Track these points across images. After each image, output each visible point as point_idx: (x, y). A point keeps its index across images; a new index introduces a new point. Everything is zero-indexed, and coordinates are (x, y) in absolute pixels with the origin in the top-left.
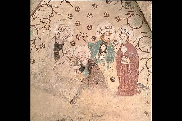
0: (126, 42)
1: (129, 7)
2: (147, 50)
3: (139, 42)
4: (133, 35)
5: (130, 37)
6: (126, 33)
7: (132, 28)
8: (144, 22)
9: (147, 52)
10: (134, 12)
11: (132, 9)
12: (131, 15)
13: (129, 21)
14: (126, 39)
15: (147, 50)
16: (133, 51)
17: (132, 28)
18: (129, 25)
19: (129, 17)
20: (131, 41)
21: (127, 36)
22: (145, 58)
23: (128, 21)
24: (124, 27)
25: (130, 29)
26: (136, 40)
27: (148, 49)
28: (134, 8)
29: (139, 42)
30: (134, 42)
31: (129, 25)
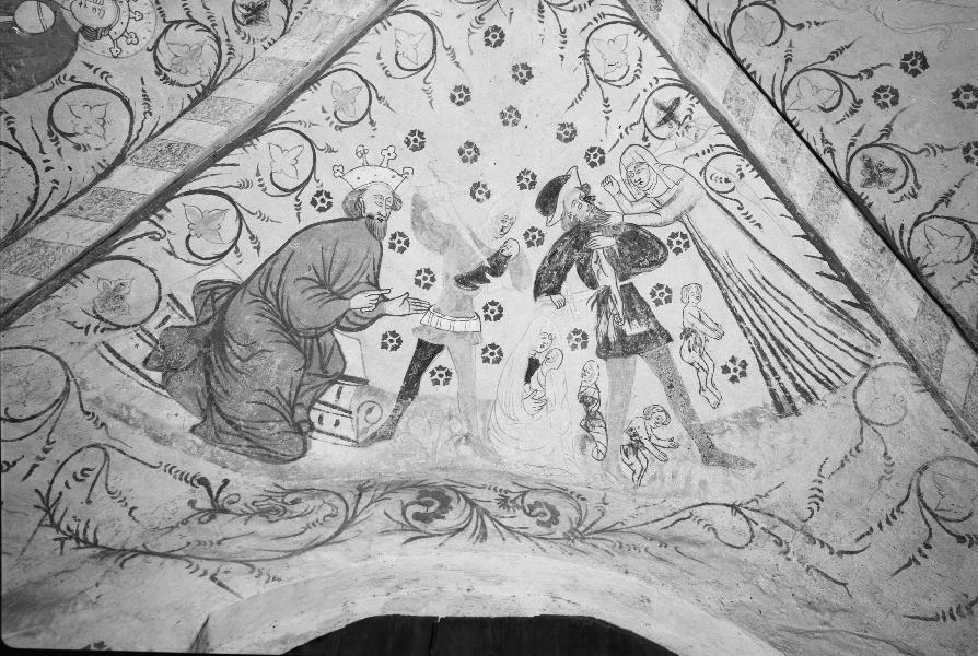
0: (76, 27)
1: (241, 20)
2: (63, 134)
3: (94, 86)
4: (124, 54)
5: (106, 41)
6: (124, 19)
7: (156, 47)
8: (197, 92)
9: (51, 134)
10: (228, 40)
11: (238, 31)
12: (209, 31)
13: (183, 25)
14: (94, 22)
15: (63, 134)
16: (35, 64)
17: (156, 47)
18: (166, 31)
19: (197, 23)
20: (87, 52)
21: (110, 28)
22: (13, 131)
23: (179, 22)
24: (151, 9)
25: (148, 36)
26: (99, 72)
27: (71, 135)
28: (243, 39)
29: (94, 86)
30: (91, 67)
31: (166, 31)
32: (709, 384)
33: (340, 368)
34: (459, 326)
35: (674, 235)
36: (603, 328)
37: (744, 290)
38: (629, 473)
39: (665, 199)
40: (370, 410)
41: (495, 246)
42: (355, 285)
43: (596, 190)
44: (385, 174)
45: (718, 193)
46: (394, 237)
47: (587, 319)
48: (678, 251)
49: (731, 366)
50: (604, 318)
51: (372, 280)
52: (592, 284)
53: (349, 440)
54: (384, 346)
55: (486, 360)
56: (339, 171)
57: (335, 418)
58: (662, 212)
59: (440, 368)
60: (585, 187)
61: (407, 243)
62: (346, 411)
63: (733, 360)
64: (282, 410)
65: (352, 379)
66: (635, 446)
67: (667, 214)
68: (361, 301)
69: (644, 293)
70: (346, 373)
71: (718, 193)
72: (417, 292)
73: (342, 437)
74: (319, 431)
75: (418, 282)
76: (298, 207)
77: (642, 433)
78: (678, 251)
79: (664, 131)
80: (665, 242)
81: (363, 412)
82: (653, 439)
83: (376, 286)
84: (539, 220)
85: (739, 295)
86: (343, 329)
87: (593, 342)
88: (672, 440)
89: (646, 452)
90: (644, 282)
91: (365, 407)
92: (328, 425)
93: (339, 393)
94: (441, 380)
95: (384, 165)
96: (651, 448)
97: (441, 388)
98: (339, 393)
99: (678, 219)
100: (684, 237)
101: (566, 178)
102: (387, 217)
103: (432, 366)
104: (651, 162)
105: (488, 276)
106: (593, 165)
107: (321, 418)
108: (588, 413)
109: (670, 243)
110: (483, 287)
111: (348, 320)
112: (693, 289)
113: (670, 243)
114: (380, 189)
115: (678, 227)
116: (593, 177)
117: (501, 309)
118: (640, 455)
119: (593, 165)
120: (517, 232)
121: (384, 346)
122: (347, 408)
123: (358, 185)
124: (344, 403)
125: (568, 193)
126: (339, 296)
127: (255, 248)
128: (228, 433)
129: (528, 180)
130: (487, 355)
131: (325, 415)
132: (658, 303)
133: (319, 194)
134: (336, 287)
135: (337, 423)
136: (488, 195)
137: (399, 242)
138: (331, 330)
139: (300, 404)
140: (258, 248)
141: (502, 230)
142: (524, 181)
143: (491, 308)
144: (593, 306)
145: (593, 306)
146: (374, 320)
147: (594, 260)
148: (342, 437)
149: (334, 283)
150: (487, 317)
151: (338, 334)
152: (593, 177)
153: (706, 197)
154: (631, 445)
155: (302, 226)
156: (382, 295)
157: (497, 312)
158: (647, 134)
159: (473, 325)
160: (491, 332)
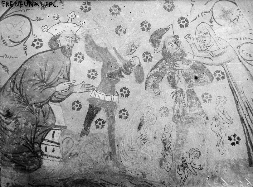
32: (221, 143)
33: (53, 122)
34: (109, 98)
35: (218, 72)
36: (177, 108)
37: (247, 106)
38: (179, 178)
39: (216, 53)
40: (68, 142)
41: (128, 58)
42: (58, 80)
43: (182, 39)
44: (70, 26)
45: (244, 59)
46: (76, 55)
47: (170, 103)
48: (218, 79)
49: (233, 138)
50: (178, 104)
51: (66, 77)
52: (174, 86)
53: (59, 158)
54: (73, 109)
55: (121, 117)
56: (46, 28)
57: (51, 148)
58: (213, 59)
59: (100, 119)
60: (176, 37)
61: (83, 58)
62: (57, 143)
63: (234, 136)
64: (28, 146)
65: (60, 127)
66: (184, 165)
67: (216, 61)
68: (60, 87)
69: (199, 95)
70: (56, 124)
71: (244, 59)
72: (90, 81)
73: (56, 157)
74: (46, 155)
75: (89, 76)
76: (25, 49)
77: (188, 161)
78: (218, 79)
79: (222, 21)
80: (213, 74)
81: (64, 143)
82: (192, 164)
83: (69, 79)
84: (149, 47)
85: (244, 108)
86: (53, 101)
87: (171, 113)
88: (200, 166)
89: (188, 169)
90: (199, 90)
91: (66, 141)
92: (49, 152)
93: (53, 134)
94: (100, 126)
95: (70, 21)
96: (191, 168)
97: (100, 130)
98: (53, 134)
99: (221, 65)
100: (223, 73)
101: (167, 29)
102: (72, 46)
103: (96, 119)
104: (213, 34)
105: (123, 74)
106: (182, 26)
107: (46, 148)
108: (165, 148)
109: (215, 74)
110: (121, 79)
111: (55, 96)
112: (223, 99)
113: (215, 74)
114: (68, 33)
115: (221, 69)
116: (181, 33)
117: (129, 92)
118: (185, 171)
119: (182, 26)
120: (139, 53)
121: (73, 109)
122: (57, 142)
123: (55, 33)
124: (56, 139)
125: (166, 37)
126: (51, 86)
127: (5, 71)
128: (5, 161)
129: (146, 26)
130: (121, 114)
131: (48, 147)
132: (205, 101)
133: (35, 40)
134: (48, 82)
135: (53, 151)
136: (125, 32)
137: (79, 57)
138: (47, 103)
139: (36, 142)
140: (8, 71)
141: (131, 51)
142: (144, 27)
143: (124, 90)
144: (173, 97)
145: (173, 97)
146: (67, 96)
147: (176, 75)
148: (56, 157)
149: (47, 80)
150: (122, 95)
151: (52, 105)
152: (181, 33)
153: (237, 59)
154: (182, 166)
155: (28, 56)
156: (71, 83)
157: (127, 93)
158: (213, 20)
159: (115, 98)
160: (123, 103)
